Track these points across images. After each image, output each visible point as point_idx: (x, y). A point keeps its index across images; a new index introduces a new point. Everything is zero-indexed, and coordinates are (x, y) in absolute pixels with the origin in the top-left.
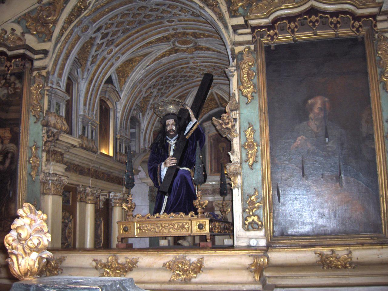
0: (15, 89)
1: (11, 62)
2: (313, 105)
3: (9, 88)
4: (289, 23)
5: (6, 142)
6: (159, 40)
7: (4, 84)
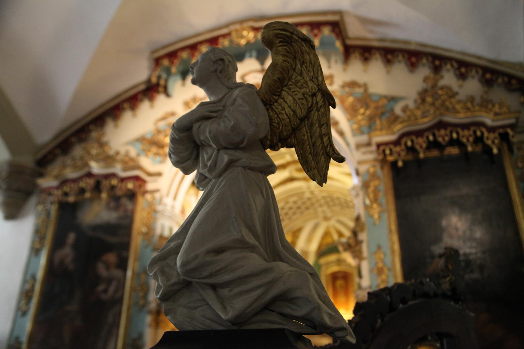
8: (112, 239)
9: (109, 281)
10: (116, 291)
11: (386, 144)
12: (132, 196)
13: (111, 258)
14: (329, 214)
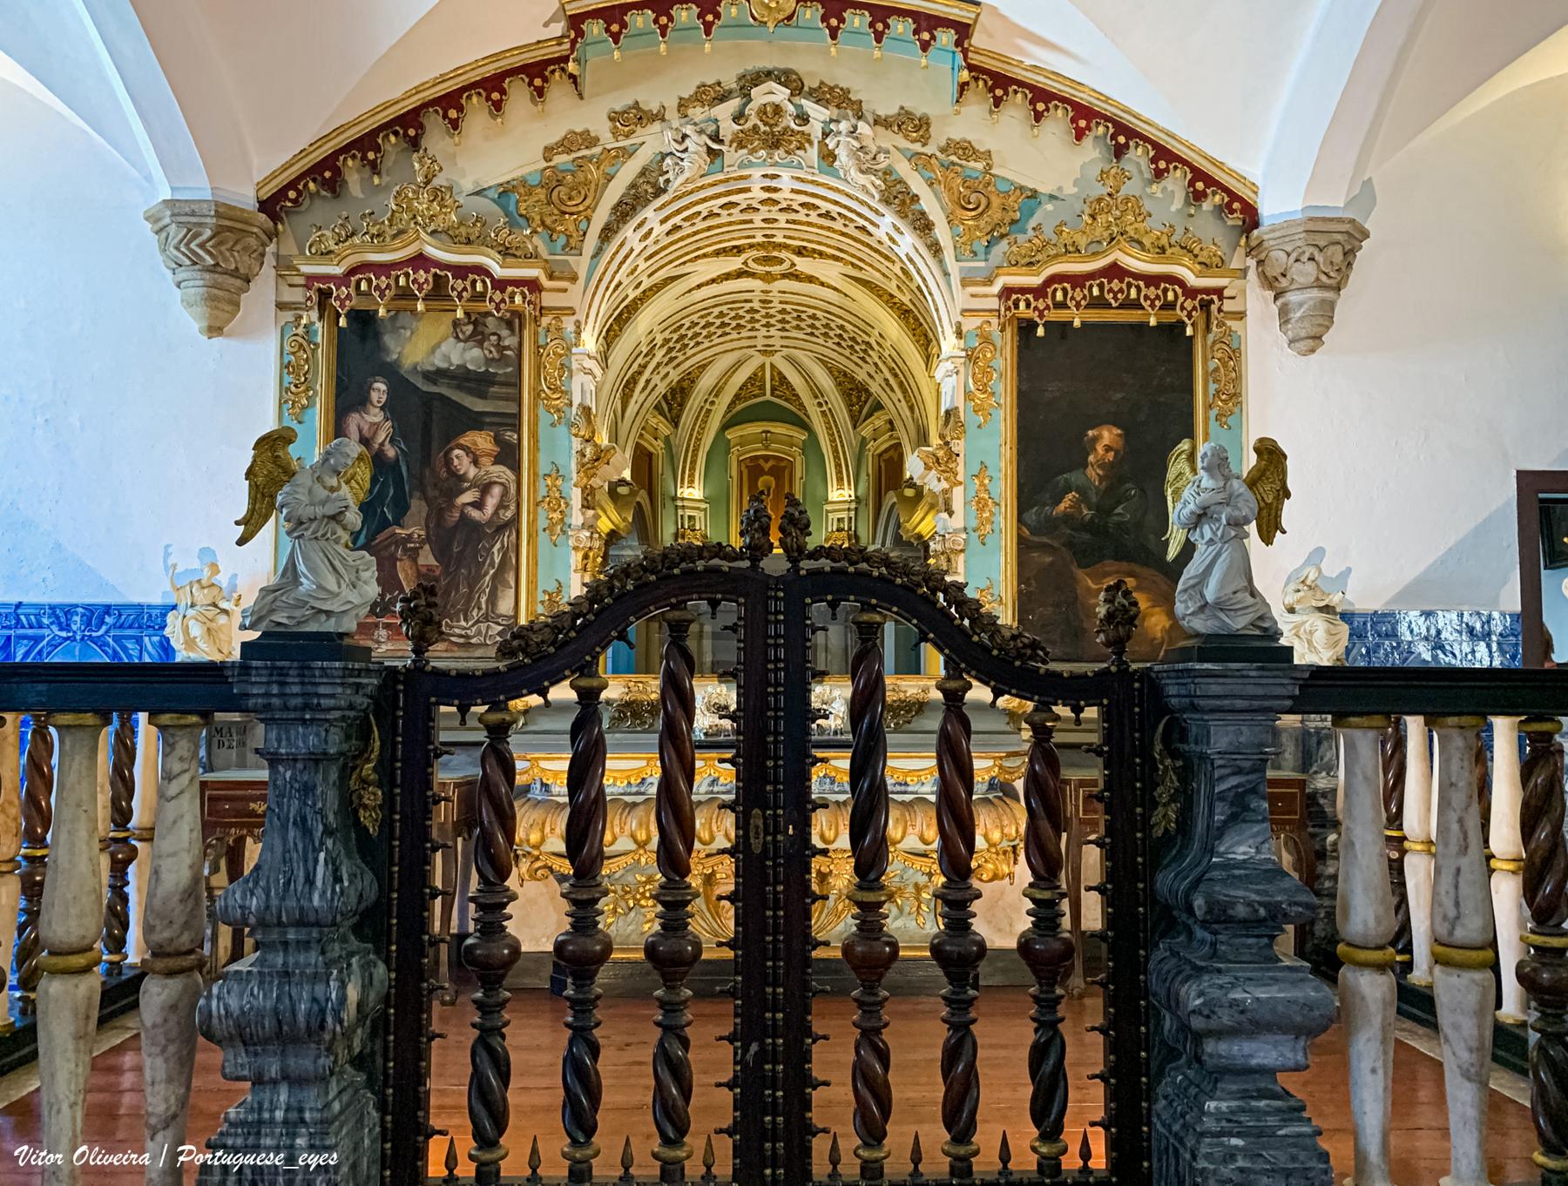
0: (501, 348)
1: (503, 291)
2: (1096, 439)
3: (486, 344)
4: (1073, 289)
5: (484, 460)
6: (717, 253)
7: (471, 336)
8: (479, 405)
9: (485, 489)
10: (502, 505)
11: (1023, 290)
12: (514, 321)
13: (482, 441)
14: (777, 342)
